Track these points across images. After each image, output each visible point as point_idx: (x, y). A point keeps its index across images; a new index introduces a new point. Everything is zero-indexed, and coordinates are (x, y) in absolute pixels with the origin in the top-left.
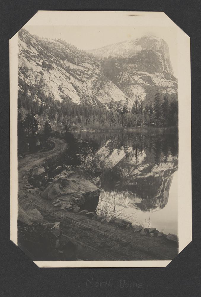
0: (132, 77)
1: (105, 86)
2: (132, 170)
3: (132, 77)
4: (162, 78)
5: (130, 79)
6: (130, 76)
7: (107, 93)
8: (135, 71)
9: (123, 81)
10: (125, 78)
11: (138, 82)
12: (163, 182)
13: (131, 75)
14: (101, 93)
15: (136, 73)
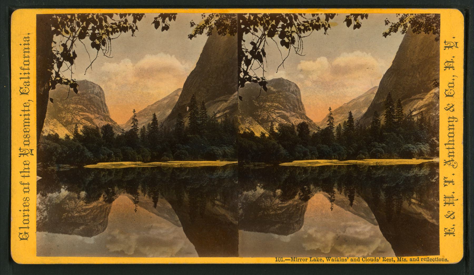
0: (75, 117)
1: (50, 124)
2: (78, 203)
3: (75, 117)
4: (101, 120)
5: (73, 118)
6: (73, 116)
7: (53, 130)
8: (77, 112)
9: (66, 120)
10: (68, 118)
11: (80, 122)
12: (105, 210)
13: (74, 115)
14: (46, 130)
15: (78, 113)
